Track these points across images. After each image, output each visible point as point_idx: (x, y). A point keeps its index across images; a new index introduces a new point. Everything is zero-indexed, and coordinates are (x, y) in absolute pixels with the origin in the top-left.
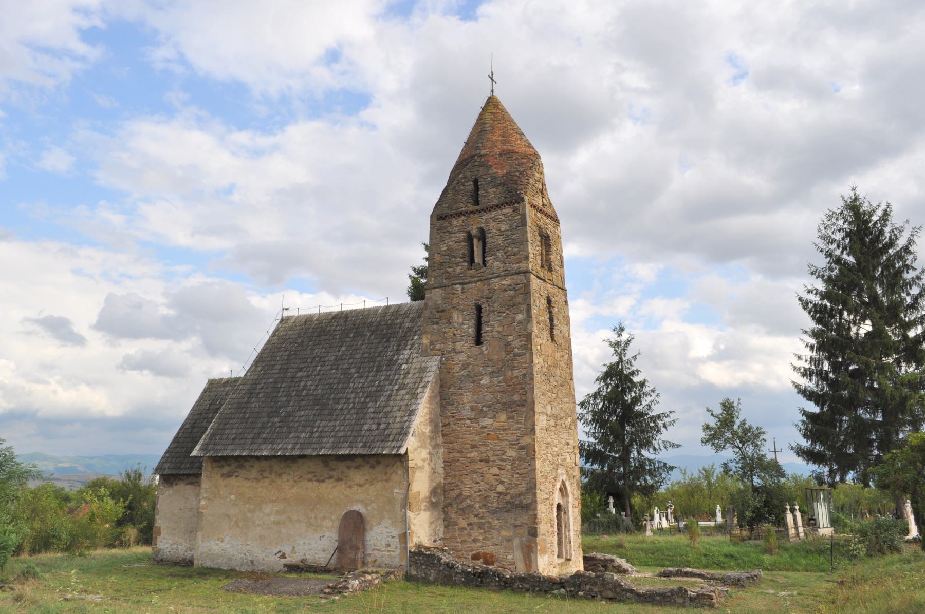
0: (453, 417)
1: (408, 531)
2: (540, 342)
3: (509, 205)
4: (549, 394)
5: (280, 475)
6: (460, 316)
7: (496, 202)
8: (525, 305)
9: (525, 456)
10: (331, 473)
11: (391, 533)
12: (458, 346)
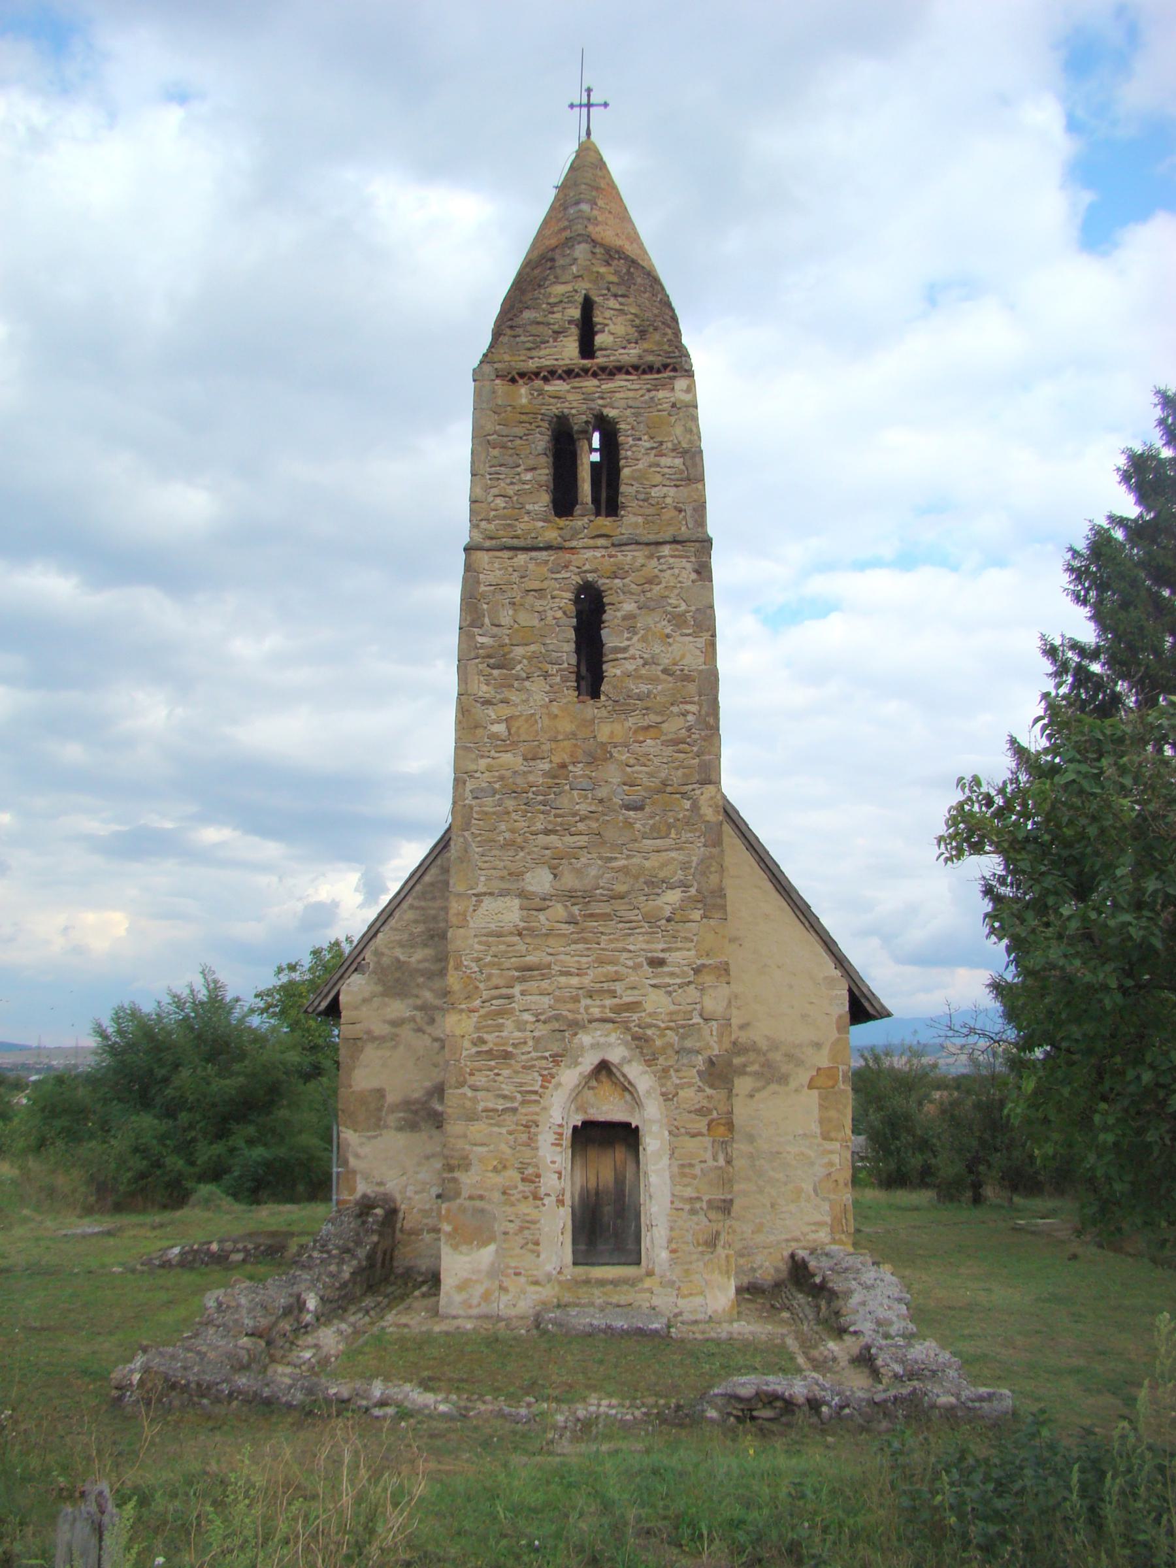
1: (335, 1170)
2: (505, 711)
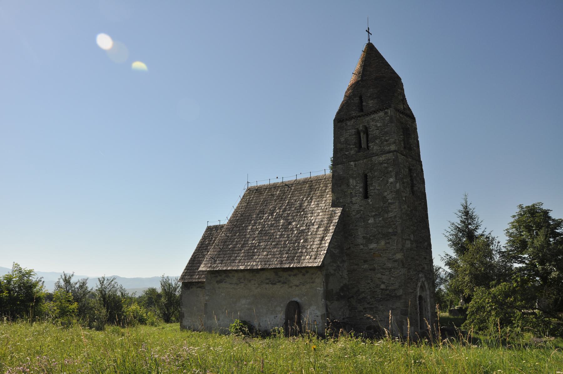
0: (352, 244)
3: (382, 111)
4: (412, 227)
5: (250, 281)
6: (354, 181)
7: (373, 109)
8: (394, 172)
9: (398, 266)
10: (279, 279)
11: (316, 314)
12: (354, 199)
